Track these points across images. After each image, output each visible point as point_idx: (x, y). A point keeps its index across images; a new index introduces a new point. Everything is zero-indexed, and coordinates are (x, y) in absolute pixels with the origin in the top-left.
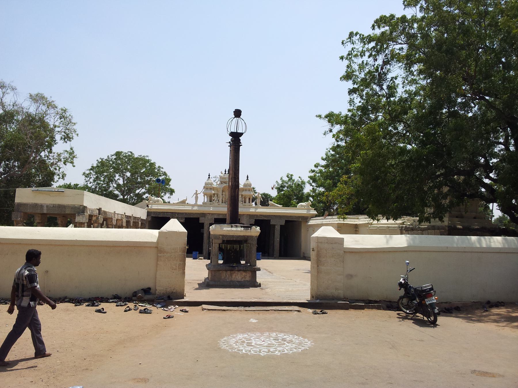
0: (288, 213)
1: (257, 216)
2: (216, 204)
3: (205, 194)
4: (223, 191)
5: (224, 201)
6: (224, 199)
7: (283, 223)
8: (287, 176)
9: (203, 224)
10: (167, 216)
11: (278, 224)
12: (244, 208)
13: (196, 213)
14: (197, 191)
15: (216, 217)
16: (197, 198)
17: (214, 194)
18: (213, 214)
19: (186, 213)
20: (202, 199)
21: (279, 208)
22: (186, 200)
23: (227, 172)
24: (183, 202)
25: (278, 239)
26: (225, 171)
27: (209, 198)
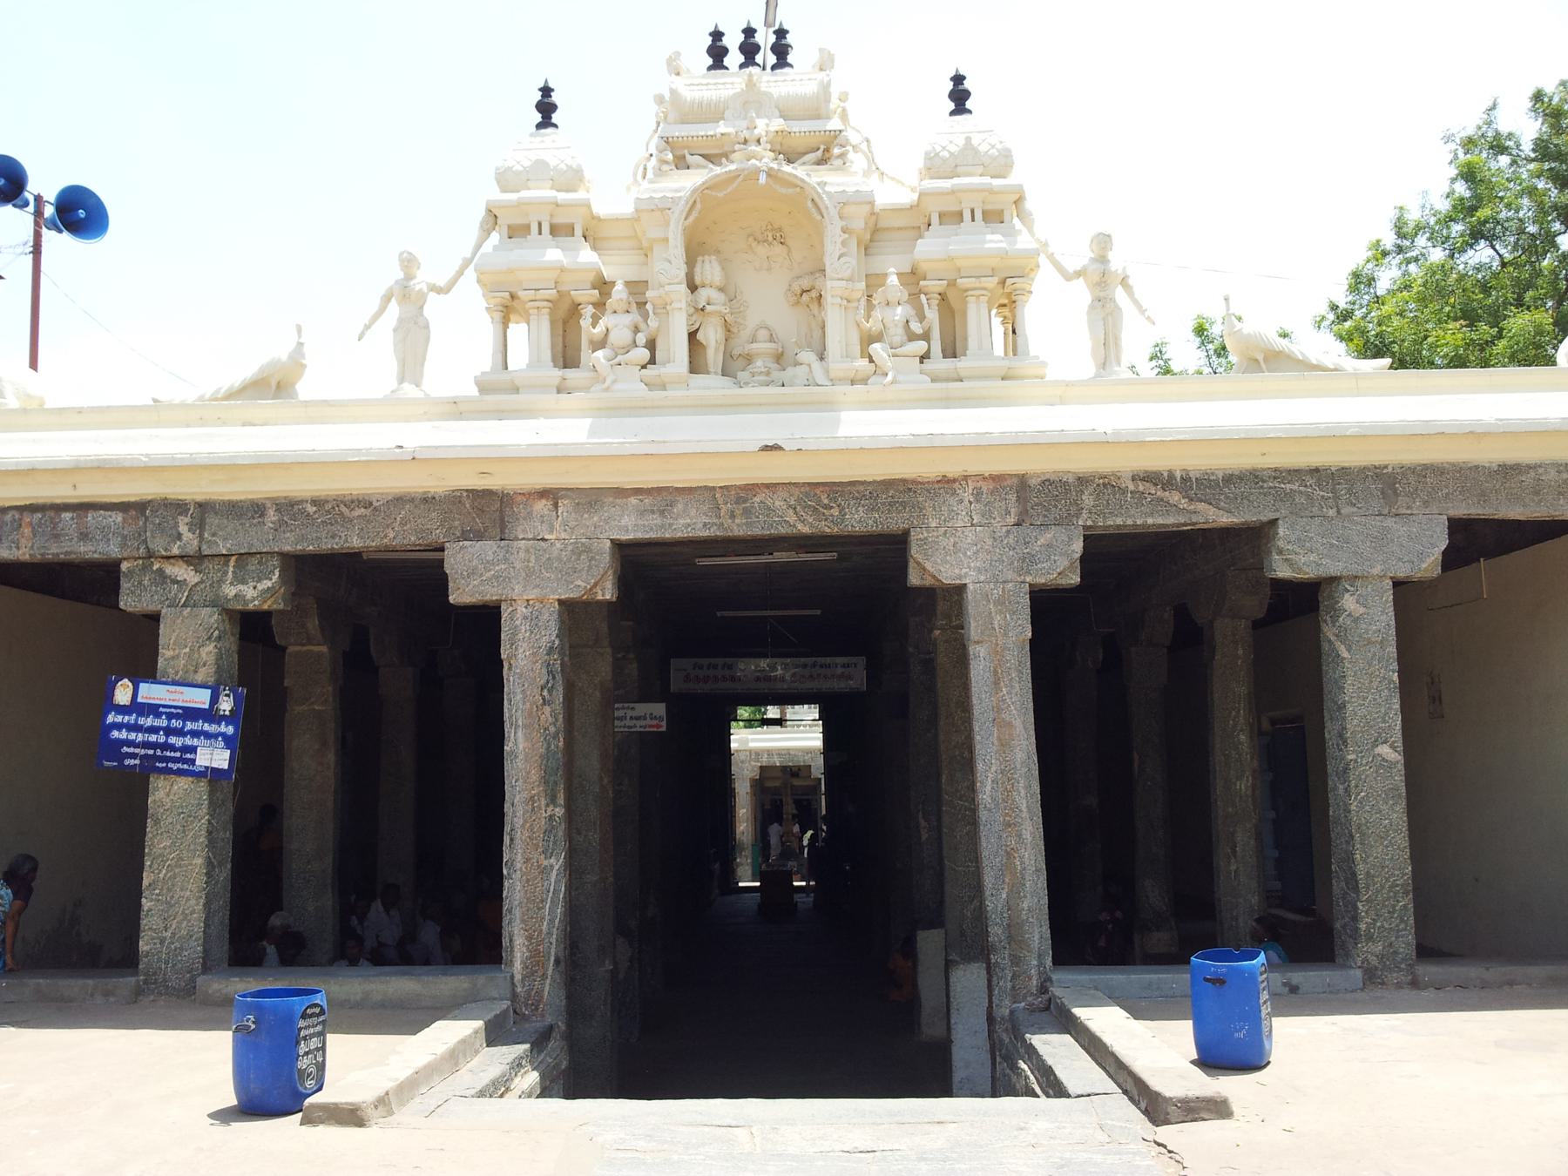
0: (1475, 434)
1: (1106, 485)
2: (630, 384)
3: (507, 309)
4: (694, 252)
5: (714, 356)
6: (711, 336)
7: (1421, 549)
8: (1200, 331)
9: (487, 618)
10: (88, 551)
11: (1366, 571)
12: (947, 402)
13: (400, 500)
14: (409, 263)
15: (632, 526)
17: (603, 286)
18: (591, 499)
19: (289, 508)
21: (1358, 386)
22: (296, 364)
23: (734, 58)
25: (1390, 753)
26: (717, 53)
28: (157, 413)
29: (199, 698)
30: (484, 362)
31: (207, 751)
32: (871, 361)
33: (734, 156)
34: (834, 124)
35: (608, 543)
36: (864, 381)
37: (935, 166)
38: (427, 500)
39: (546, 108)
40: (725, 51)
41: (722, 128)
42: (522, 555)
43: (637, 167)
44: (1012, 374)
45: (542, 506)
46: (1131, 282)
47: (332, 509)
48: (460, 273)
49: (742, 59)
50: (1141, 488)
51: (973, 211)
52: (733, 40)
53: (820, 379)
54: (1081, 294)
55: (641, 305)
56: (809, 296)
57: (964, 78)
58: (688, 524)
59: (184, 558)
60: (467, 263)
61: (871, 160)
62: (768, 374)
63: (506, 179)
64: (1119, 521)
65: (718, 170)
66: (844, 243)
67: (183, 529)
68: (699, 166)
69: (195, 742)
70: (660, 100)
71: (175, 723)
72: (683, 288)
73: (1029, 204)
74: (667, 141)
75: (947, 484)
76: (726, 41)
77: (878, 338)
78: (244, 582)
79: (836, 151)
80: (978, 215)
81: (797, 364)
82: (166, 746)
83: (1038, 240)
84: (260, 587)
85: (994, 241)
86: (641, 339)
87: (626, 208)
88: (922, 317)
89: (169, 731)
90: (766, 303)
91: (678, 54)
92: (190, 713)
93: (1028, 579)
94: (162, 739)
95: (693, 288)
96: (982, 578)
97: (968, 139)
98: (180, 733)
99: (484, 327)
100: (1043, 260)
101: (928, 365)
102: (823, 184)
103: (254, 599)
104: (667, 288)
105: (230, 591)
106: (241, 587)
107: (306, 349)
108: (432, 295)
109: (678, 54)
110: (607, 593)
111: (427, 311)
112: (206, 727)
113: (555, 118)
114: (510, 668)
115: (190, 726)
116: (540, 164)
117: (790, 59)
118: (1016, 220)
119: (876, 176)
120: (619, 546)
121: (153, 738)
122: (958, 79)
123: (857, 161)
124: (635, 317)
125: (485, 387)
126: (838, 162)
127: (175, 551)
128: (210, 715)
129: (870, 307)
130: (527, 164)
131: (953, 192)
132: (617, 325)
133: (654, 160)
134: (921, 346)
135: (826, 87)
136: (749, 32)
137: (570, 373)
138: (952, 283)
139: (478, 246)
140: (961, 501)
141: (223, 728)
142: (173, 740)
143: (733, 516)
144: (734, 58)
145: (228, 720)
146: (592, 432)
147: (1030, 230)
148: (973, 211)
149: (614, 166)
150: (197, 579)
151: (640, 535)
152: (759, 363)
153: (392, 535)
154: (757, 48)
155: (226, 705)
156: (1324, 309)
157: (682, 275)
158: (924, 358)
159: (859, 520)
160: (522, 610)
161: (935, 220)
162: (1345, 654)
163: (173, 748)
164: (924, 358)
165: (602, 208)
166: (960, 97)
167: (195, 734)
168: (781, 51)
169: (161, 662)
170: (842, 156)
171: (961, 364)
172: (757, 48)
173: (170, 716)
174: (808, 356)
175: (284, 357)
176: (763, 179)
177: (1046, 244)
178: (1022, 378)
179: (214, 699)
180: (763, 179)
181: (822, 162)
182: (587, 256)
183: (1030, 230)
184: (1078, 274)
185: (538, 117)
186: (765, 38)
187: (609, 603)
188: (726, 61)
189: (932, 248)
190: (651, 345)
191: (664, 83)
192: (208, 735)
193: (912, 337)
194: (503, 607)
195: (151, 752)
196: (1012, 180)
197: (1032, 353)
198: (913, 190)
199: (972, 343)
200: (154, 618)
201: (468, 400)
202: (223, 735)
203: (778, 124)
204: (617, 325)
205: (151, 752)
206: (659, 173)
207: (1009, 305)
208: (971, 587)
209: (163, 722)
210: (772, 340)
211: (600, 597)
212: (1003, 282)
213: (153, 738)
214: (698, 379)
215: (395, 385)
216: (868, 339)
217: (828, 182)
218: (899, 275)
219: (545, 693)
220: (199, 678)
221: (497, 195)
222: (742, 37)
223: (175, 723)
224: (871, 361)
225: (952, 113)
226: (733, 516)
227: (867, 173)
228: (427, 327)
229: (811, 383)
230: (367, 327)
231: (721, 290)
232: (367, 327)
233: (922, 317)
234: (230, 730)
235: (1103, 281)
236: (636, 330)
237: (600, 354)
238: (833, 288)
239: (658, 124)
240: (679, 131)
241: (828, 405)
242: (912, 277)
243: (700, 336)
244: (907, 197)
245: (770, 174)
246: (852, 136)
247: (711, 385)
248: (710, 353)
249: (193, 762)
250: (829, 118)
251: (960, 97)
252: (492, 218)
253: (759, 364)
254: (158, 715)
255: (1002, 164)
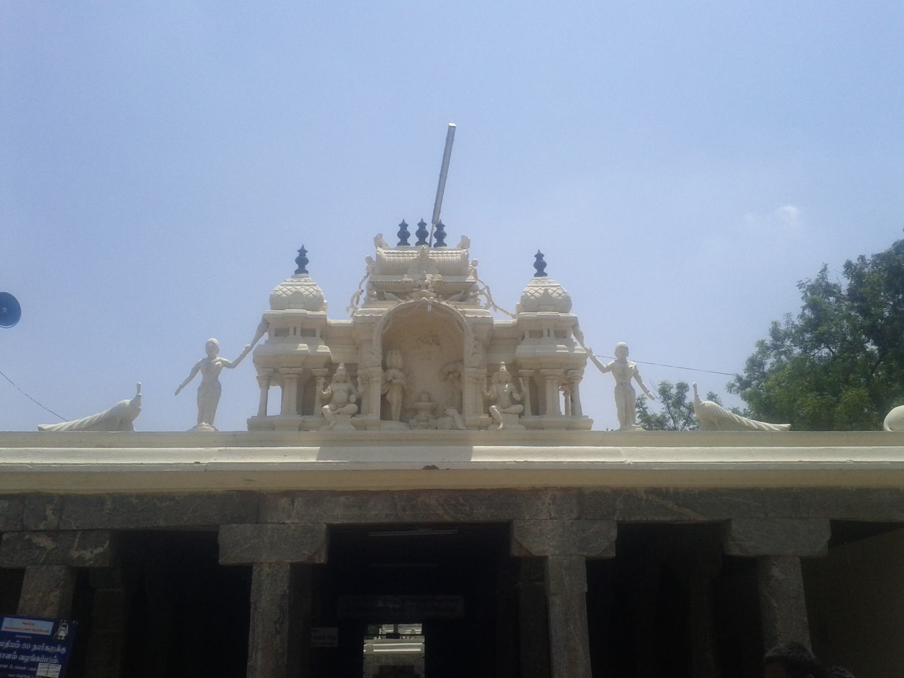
2: (345, 427)
5: (395, 409)
6: (395, 397)
13: (193, 497)
15: (340, 515)
16: (210, 397)
17: (331, 366)
18: (315, 497)
20: (244, 397)
22: (135, 408)
23: (413, 239)
24: (117, 424)
26: (403, 235)
27: (293, 390)
28: (41, 438)
29: (44, 628)
30: (253, 410)
31: (46, 665)
32: (490, 415)
33: (413, 294)
34: (471, 279)
35: (325, 526)
36: (486, 427)
37: (527, 303)
38: (211, 497)
39: (302, 261)
40: (408, 235)
41: (406, 278)
42: (269, 533)
43: (353, 297)
44: (574, 427)
45: (284, 502)
46: (640, 374)
47: (149, 501)
48: (243, 356)
49: (417, 240)
50: (650, 498)
51: (549, 331)
52: (413, 229)
53: (460, 426)
54: (610, 381)
55: (354, 378)
56: (453, 375)
57: (543, 255)
58: (377, 514)
59: (48, 532)
60: (248, 350)
61: (489, 299)
62: (427, 421)
63: (276, 301)
64: (638, 518)
65: (403, 302)
66: (475, 347)
67: (49, 512)
68: (391, 299)
69: (38, 659)
70: (369, 260)
71: (26, 646)
72: (380, 369)
73: (582, 328)
74: (373, 285)
75: (535, 493)
76: (409, 229)
77: (495, 402)
78: (85, 548)
79: (471, 294)
80: (552, 333)
81: (444, 415)
82: (18, 662)
83: (586, 349)
84: (95, 552)
85: (561, 348)
86: (353, 398)
87: (346, 320)
88: (519, 390)
89: (21, 652)
90: (427, 377)
91: (381, 235)
92: (37, 639)
93: (585, 553)
94: (15, 657)
95: (385, 368)
96: (557, 552)
97: (546, 291)
98: (28, 653)
99: (255, 391)
100: (589, 360)
101: (523, 419)
102: (465, 312)
103: (90, 560)
104: (371, 369)
105: (75, 554)
106: (82, 552)
107: (142, 400)
108: (224, 369)
109: (381, 235)
110: (322, 559)
111: (221, 378)
112: (47, 649)
113: (307, 267)
114: (255, 609)
115: (35, 648)
116: (297, 294)
117: (445, 241)
118: (573, 337)
119: (492, 308)
120: (330, 527)
121: (9, 656)
122: (539, 256)
123: (483, 299)
124: (349, 385)
125: (254, 425)
126: (472, 300)
127: (42, 527)
128: (51, 640)
129: (489, 384)
130: (289, 293)
131: (538, 320)
132: (338, 390)
133: (364, 295)
134: (520, 407)
135: (465, 258)
136: (422, 225)
137: (308, 418)
138: (537, 371)
139: (255, 341)
140: (544, 503)
141: (58, 649)
142: (23, 658)
143: (404, 510)
144: (413, 239)
145: (63, 643)
146: (320, 455)
147: (582, 345)
148: (549, 331)
149: (342, 297)
150: (53, 546)
151: (345, 521)
152: (423, 414)
153: (186, 519)
154: (426, 234)
155: (63, 633)
156: (732, 379)
157: (380, 361)
158: (521, 415)
159: (481, 514)
160: (267, 570)
161: (527, 335)
162: (775, 605)
163: (21, 663)
164: (521, 415)
165: (332, 321)
166: (540, 266)
167: (38, 653)
168: (440, 235)
169: (21, 603)
170: (475, 297)
171: (545, 419)
172: (426, 234)
173: (23, 641)
174: (452, 411)
175: (128, 401)
176: (430, 308)
177: (590, 351)
178: (578, 428)
179: (55, 629)
180: (430, 308)
181: (462, 300)
182: (323, 349)
183: (582, 345)
184: (609, 369)
185: (296, 267)
186: (430, 228)
187: (322, 565)
188: (409, 240)
189: (525, 350)
190: (359, 402)
191: (372, 252)
192: (47, 654)
193: (514, 402)
194: (254, 568)
195: (6, 666)
196: (572, 314)
197: (584, 414)
198: (514, 317)
199: (549, 406)
200: (21, 572)
201: (241, 433)
202: (58, 654)
203: (438, 277)
204: (338, 390)
205: (6, 666)
206: (368, 302)
207: (570, 384)
208: (550, 558)
209: (17, 645)
210: (430, 400)
211: (317, 562)
212: (566, 372)
213: (9, 656)
214: (387, 424)
215: (196, 424)
216: (488, 402)
217: (469, 312)
218: (506, 365)
219: (278, 626)
220: (46, 614)
221: (269, 311)
222: (418, 228)
223: (26, 646)
224: (490, 415)
225: (536, 275)
226: (404, 510)
227: (487, 307)
228: (220, 388)
229: (454, 427)
230: (182, 387)
231: (401, 370)
232: (182, 387)
233: (519, 390)
234: (64, 650)
235: (623, 373)
236: (350, 393)
237: (327, 407)
238: (469, 372)
239: (368, 274)
240: (381, 279)
241: (467, 442)
242: (514, 367)
243: (388, 397)
244: (511, 321)
245: (434, 305)
246: (481, 287)
247: (394, 427)
248: (394, 408)
249: (34, 673)
250: (468, 275)
251: (540, 266)
252: (266, 324)
253: (423, 415)
254: (14, 640)
255: (565, 304)
